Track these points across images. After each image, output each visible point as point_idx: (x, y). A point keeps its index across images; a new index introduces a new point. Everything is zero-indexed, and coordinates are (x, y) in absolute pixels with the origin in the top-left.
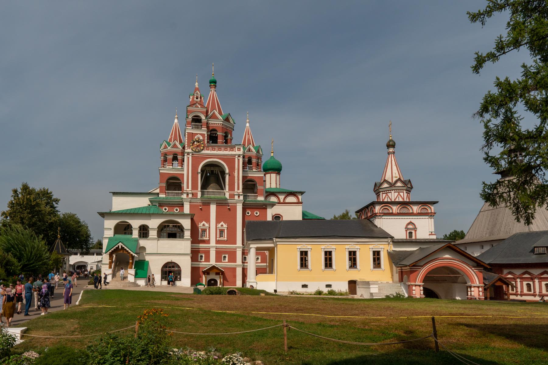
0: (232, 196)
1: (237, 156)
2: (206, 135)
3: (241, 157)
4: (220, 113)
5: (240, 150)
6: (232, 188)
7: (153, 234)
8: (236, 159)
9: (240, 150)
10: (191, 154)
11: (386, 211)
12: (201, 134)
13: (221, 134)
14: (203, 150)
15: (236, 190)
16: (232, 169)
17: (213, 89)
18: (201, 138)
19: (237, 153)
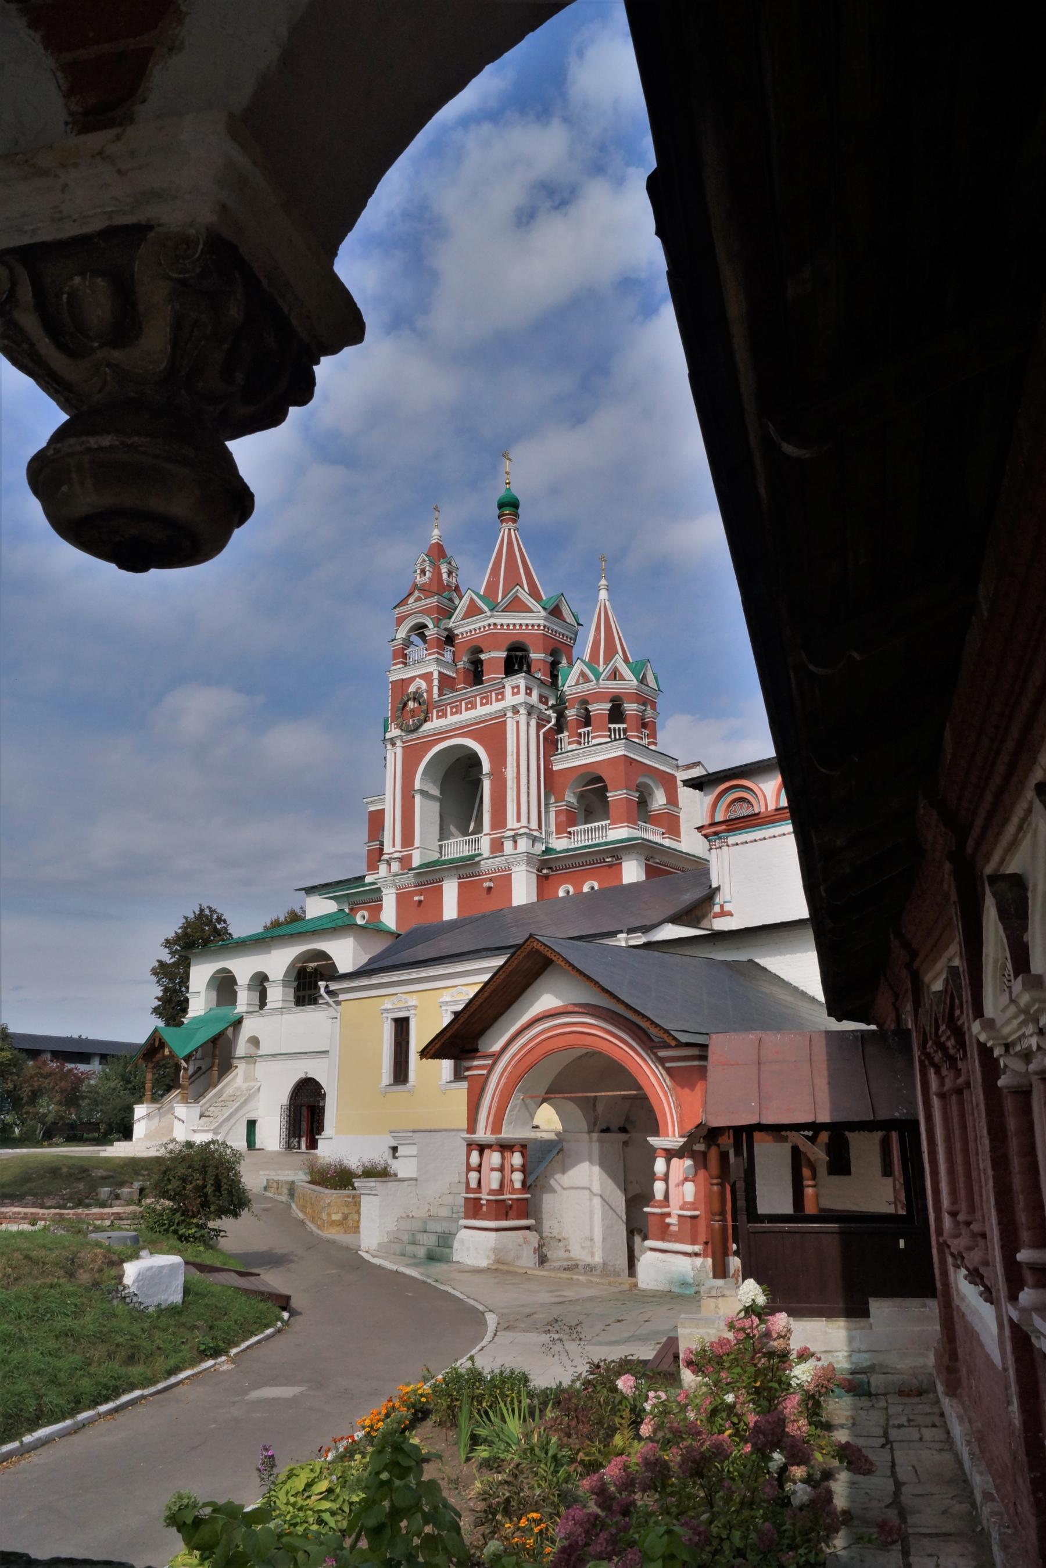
0: (497, 846)
1: (509, 714)
2: (436, 675)
3: (523, 711)
4: (535, 594)
5: (518, 693)
6: (499, 821)
7: (276, 994)
8: (509, 721)
9: (518, 693)
10: (399, 743)
11: (743, 811)
12: (421, 676)
13: (541, 656)
14: (426, 721)
15: (511, 822)
16: (499, 757)
17: (506, 527)
18: (424, 686)
19: (510, 700)
